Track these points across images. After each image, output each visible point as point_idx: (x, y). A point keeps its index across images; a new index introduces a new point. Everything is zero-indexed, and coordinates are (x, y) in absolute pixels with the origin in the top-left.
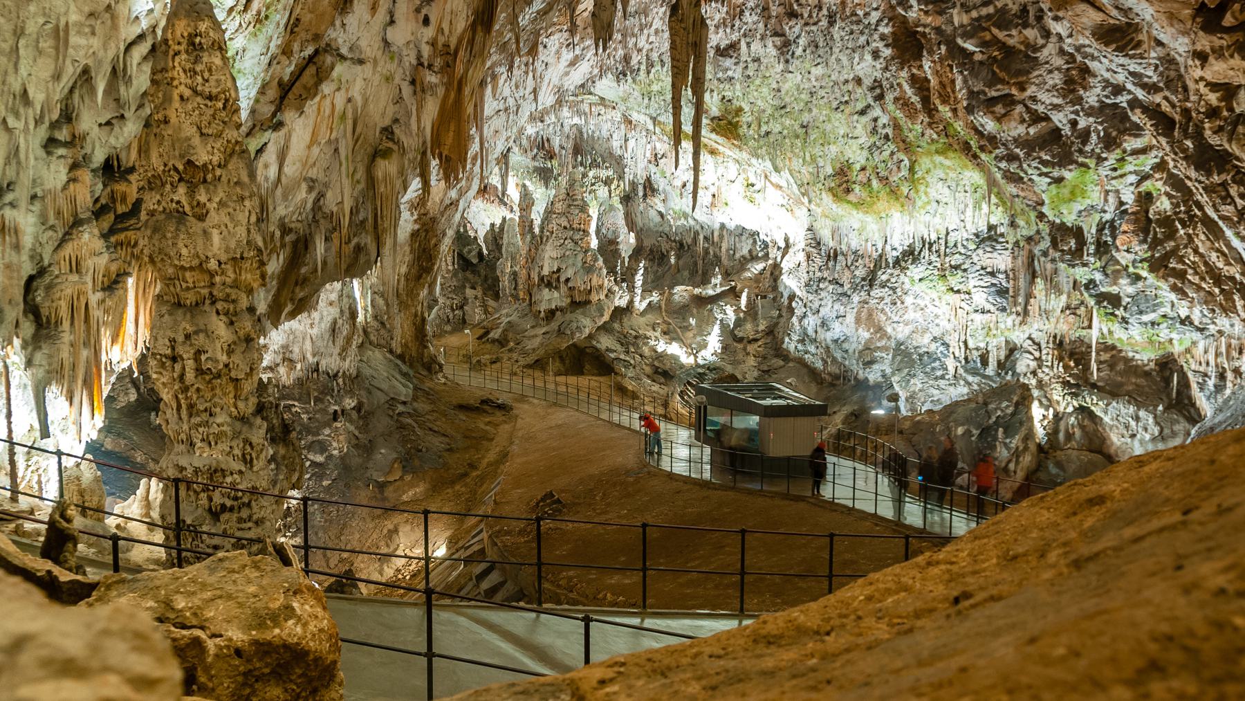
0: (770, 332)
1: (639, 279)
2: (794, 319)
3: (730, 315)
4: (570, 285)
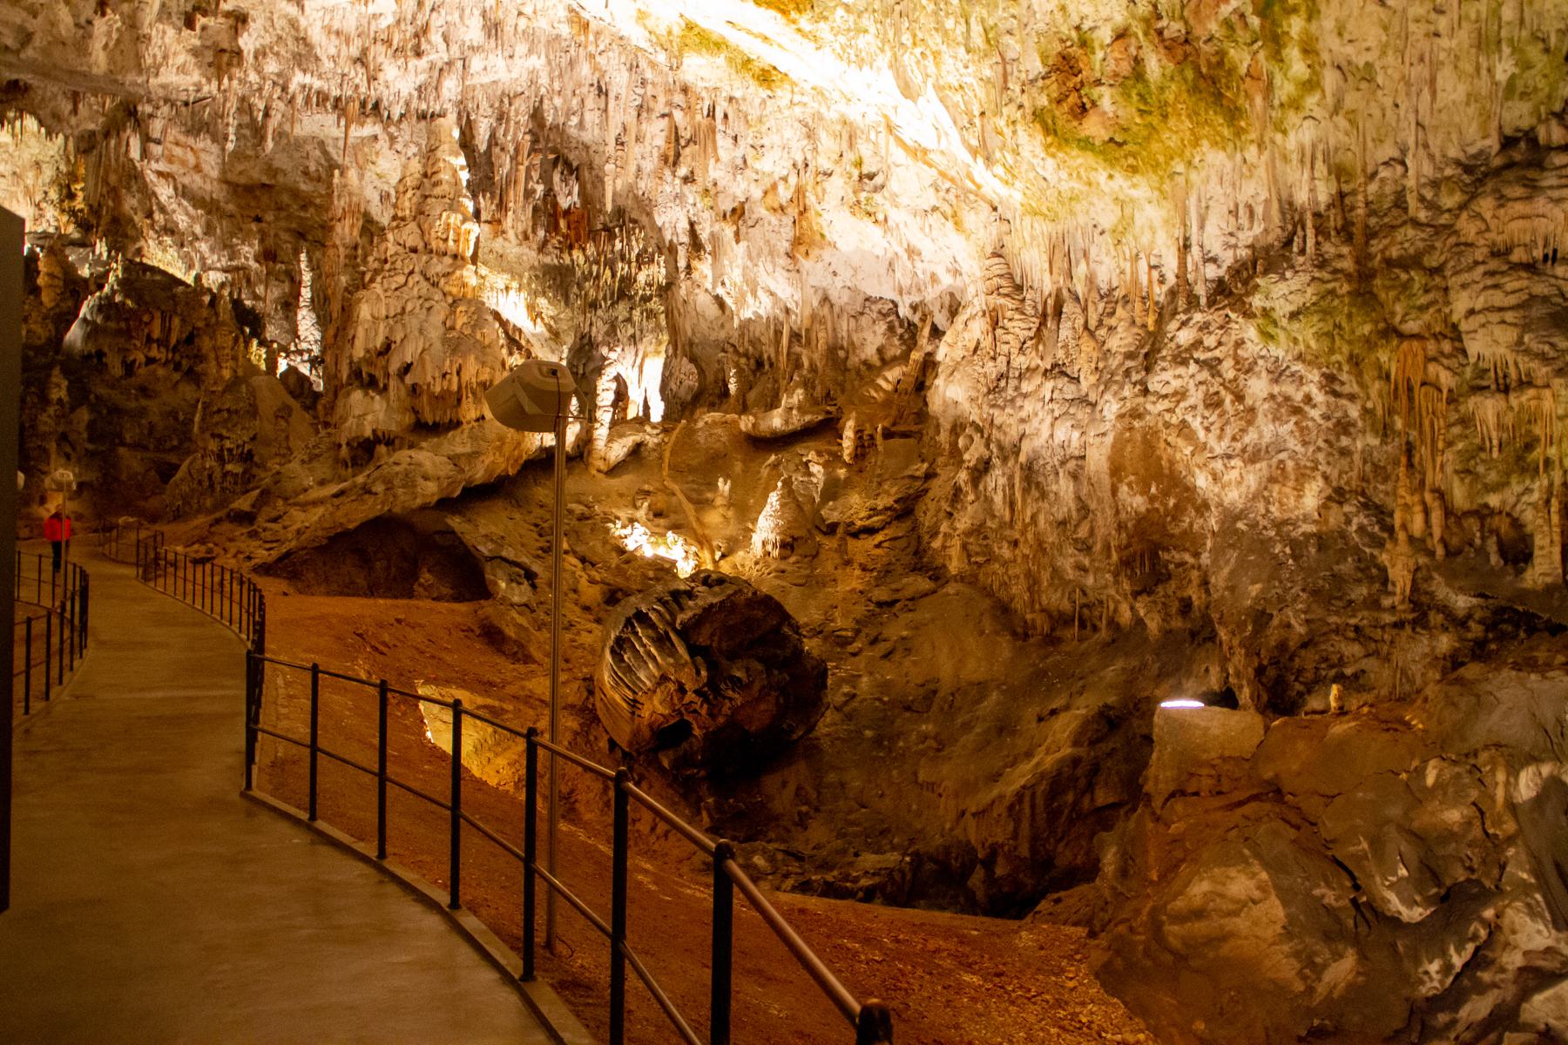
0: (905, 510)
4: (409, 379)
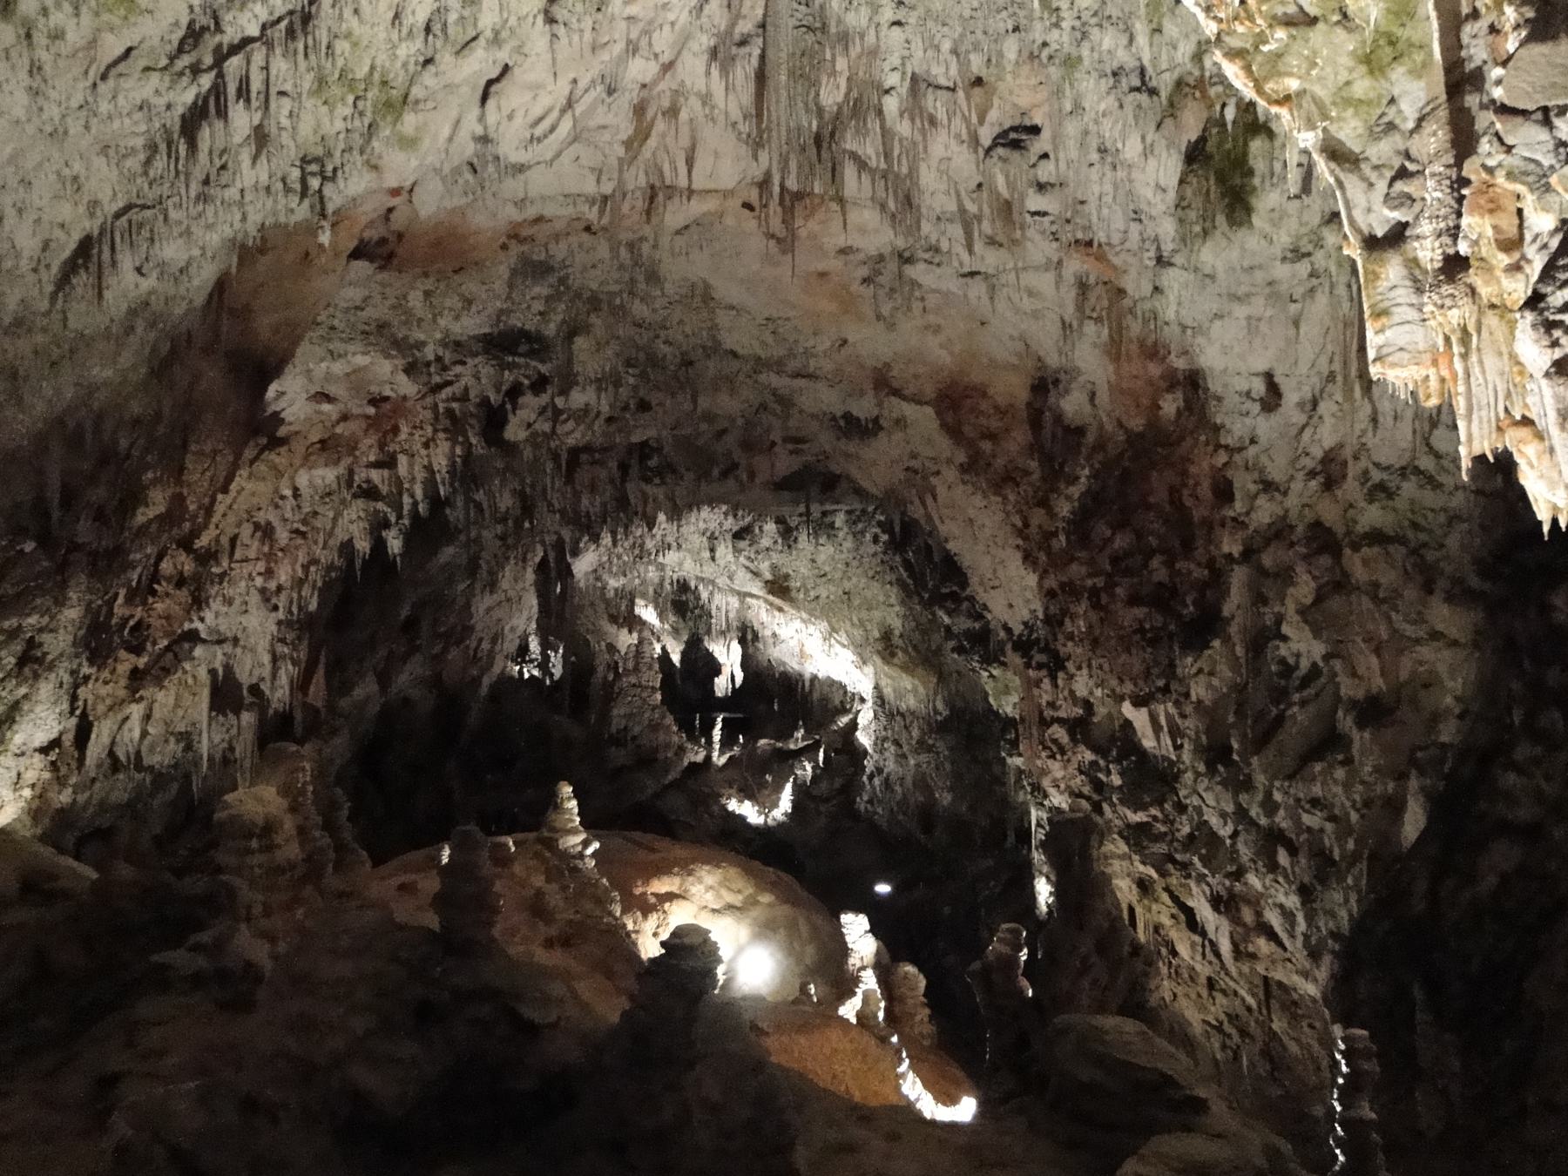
1: (717, 734)
2: (865, 778)
3: (807, 770)
